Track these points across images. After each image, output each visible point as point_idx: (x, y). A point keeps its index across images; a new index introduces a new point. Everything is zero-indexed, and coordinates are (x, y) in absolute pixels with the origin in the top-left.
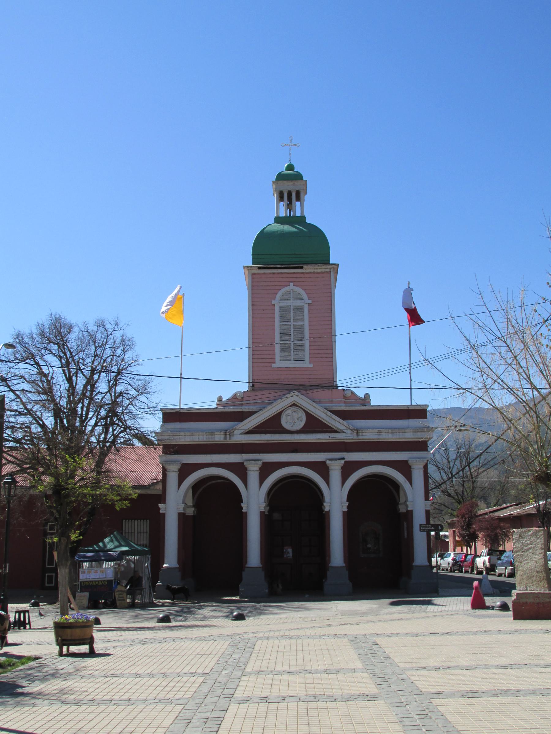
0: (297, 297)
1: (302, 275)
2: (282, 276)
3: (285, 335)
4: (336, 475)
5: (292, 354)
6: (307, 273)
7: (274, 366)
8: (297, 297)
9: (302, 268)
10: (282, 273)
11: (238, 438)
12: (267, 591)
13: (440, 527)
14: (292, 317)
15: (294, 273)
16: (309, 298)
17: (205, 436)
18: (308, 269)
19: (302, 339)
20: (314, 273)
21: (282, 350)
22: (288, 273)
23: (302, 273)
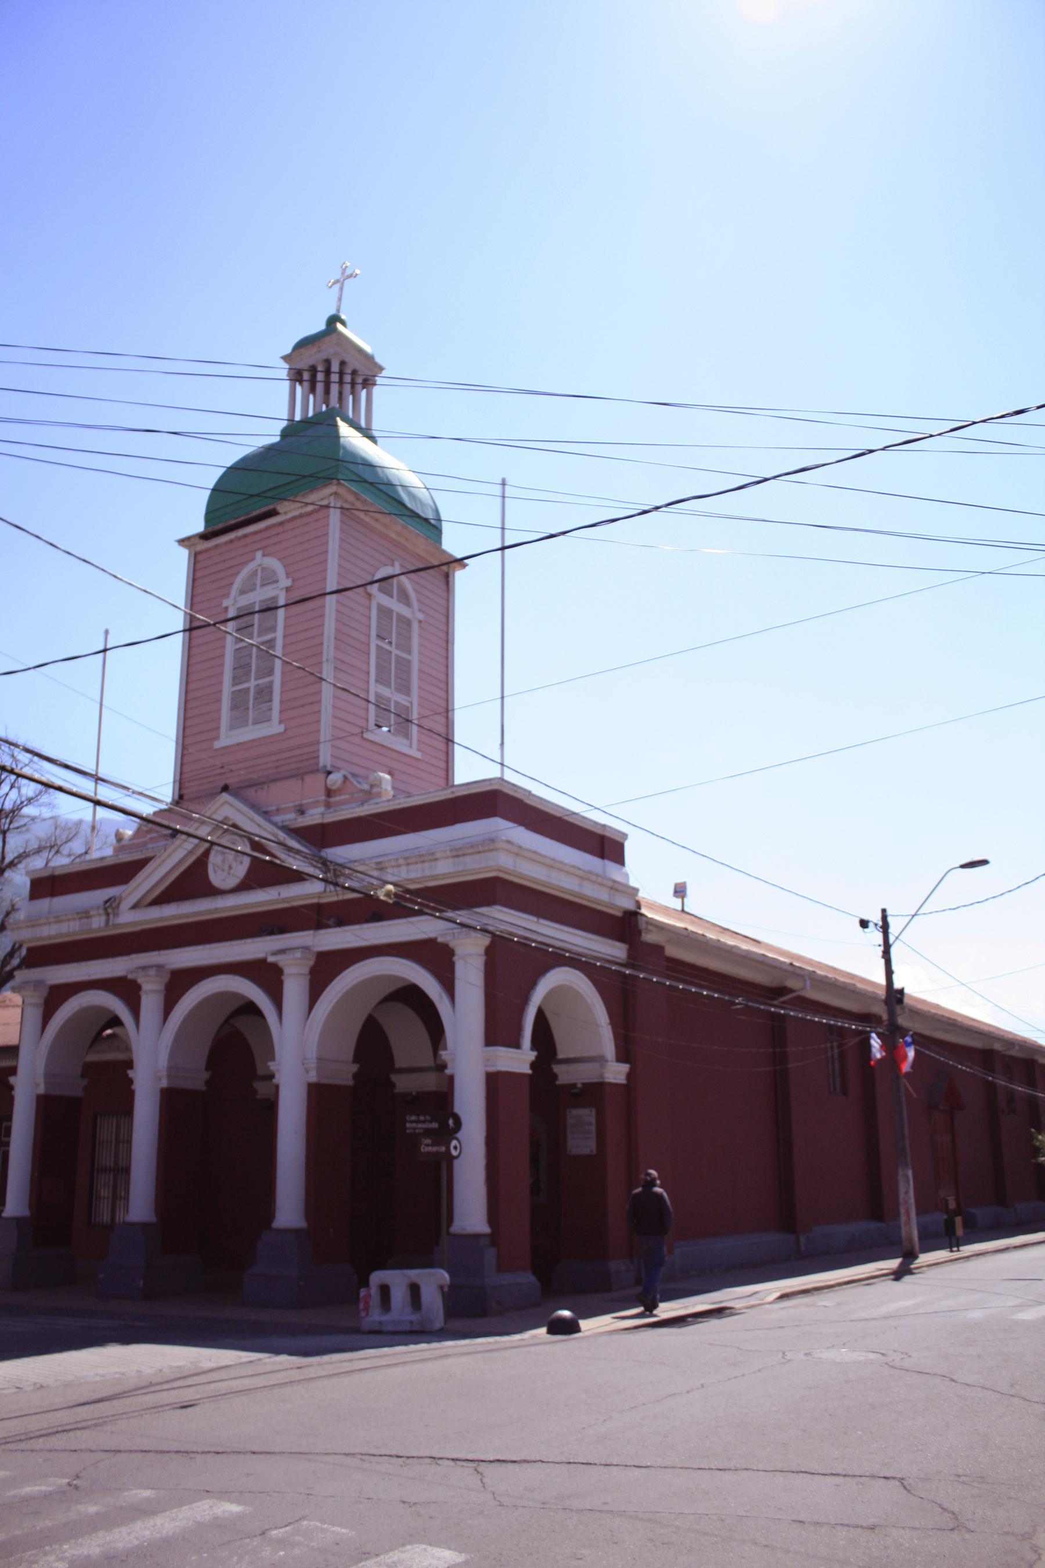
0: (270, 579)
1: (280, 529)
2: (247, 540)
3: (242, 671)
4: (294, 989)
5: (251, 712)
6: (294, 518)
7: (217, 745)
8: (270, 579)
9: (274, 513)
10: (245, 536)
11: (130, 918)
12: (141, 1283)
13: (451, 1122)
14: (256, 627)
15: (267, 528)
16: (288, 575)
17: (78, 922)
18: (288, 510)
19: (271, 672)
20: (301, 516)
21: (234, 707)
22: (256, 533)
23: (281, 524)
